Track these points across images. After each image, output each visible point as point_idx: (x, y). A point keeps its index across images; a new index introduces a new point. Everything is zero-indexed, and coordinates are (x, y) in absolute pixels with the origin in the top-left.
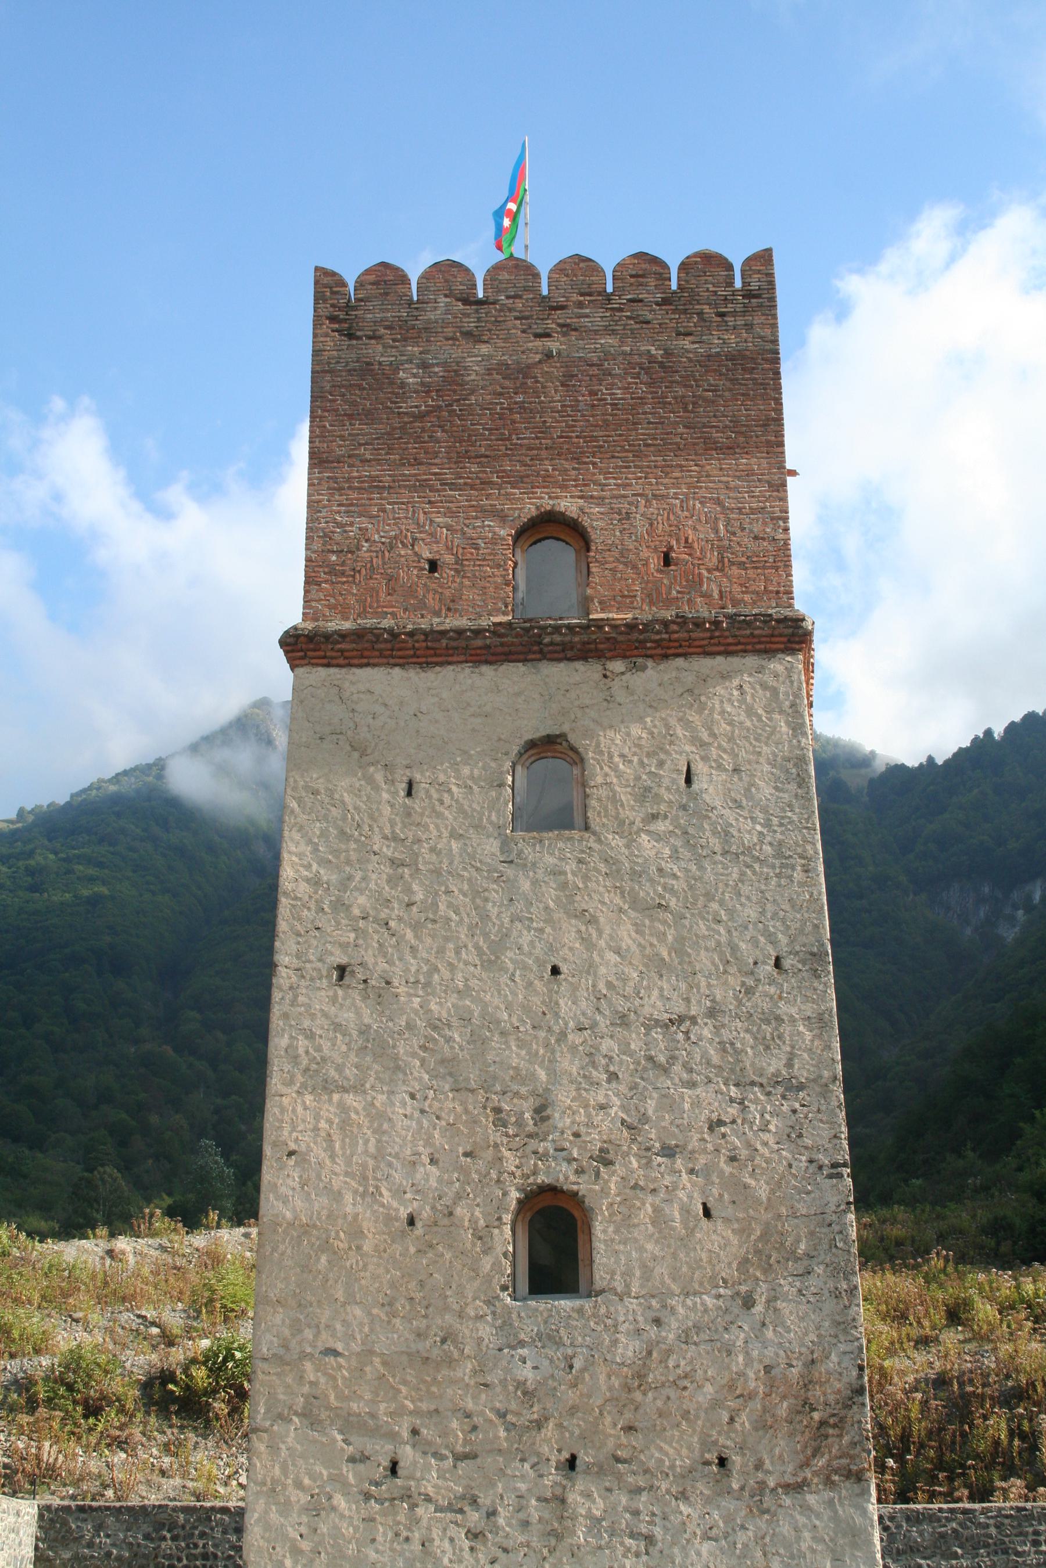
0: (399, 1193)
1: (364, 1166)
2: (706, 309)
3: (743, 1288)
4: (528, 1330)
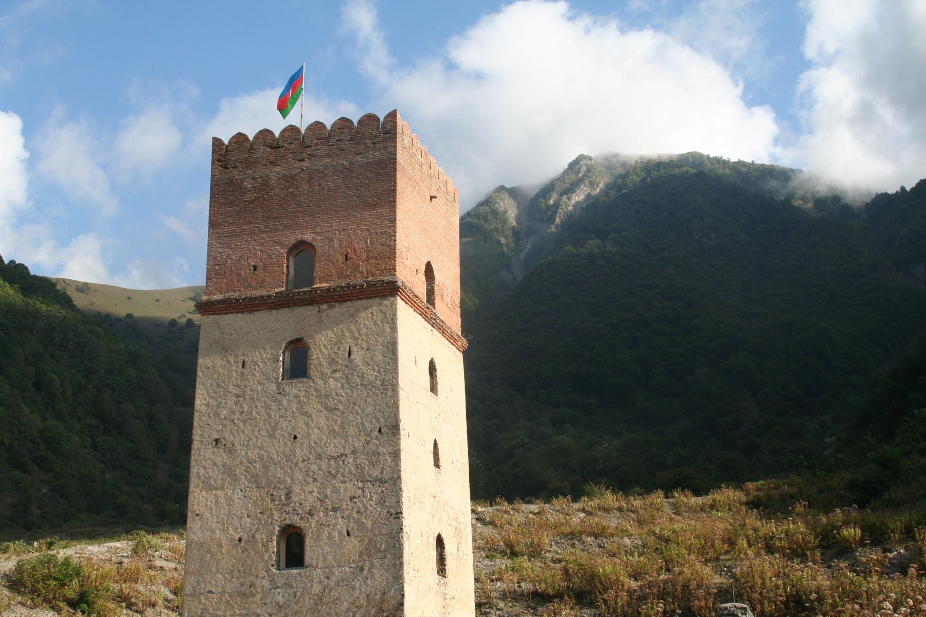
0: (235, 529)
2: (368, 141)
3: (360, 564)
4: (280, 582)
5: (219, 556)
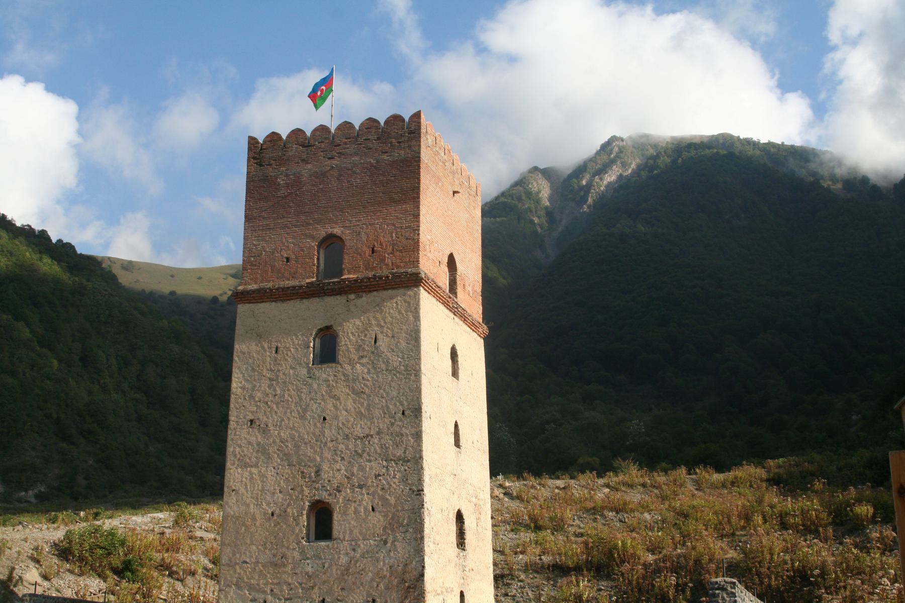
0: (268, 504)
1: (257, 494)
2: (394, 140)
3: (384, 537)
5: (253, 529)
